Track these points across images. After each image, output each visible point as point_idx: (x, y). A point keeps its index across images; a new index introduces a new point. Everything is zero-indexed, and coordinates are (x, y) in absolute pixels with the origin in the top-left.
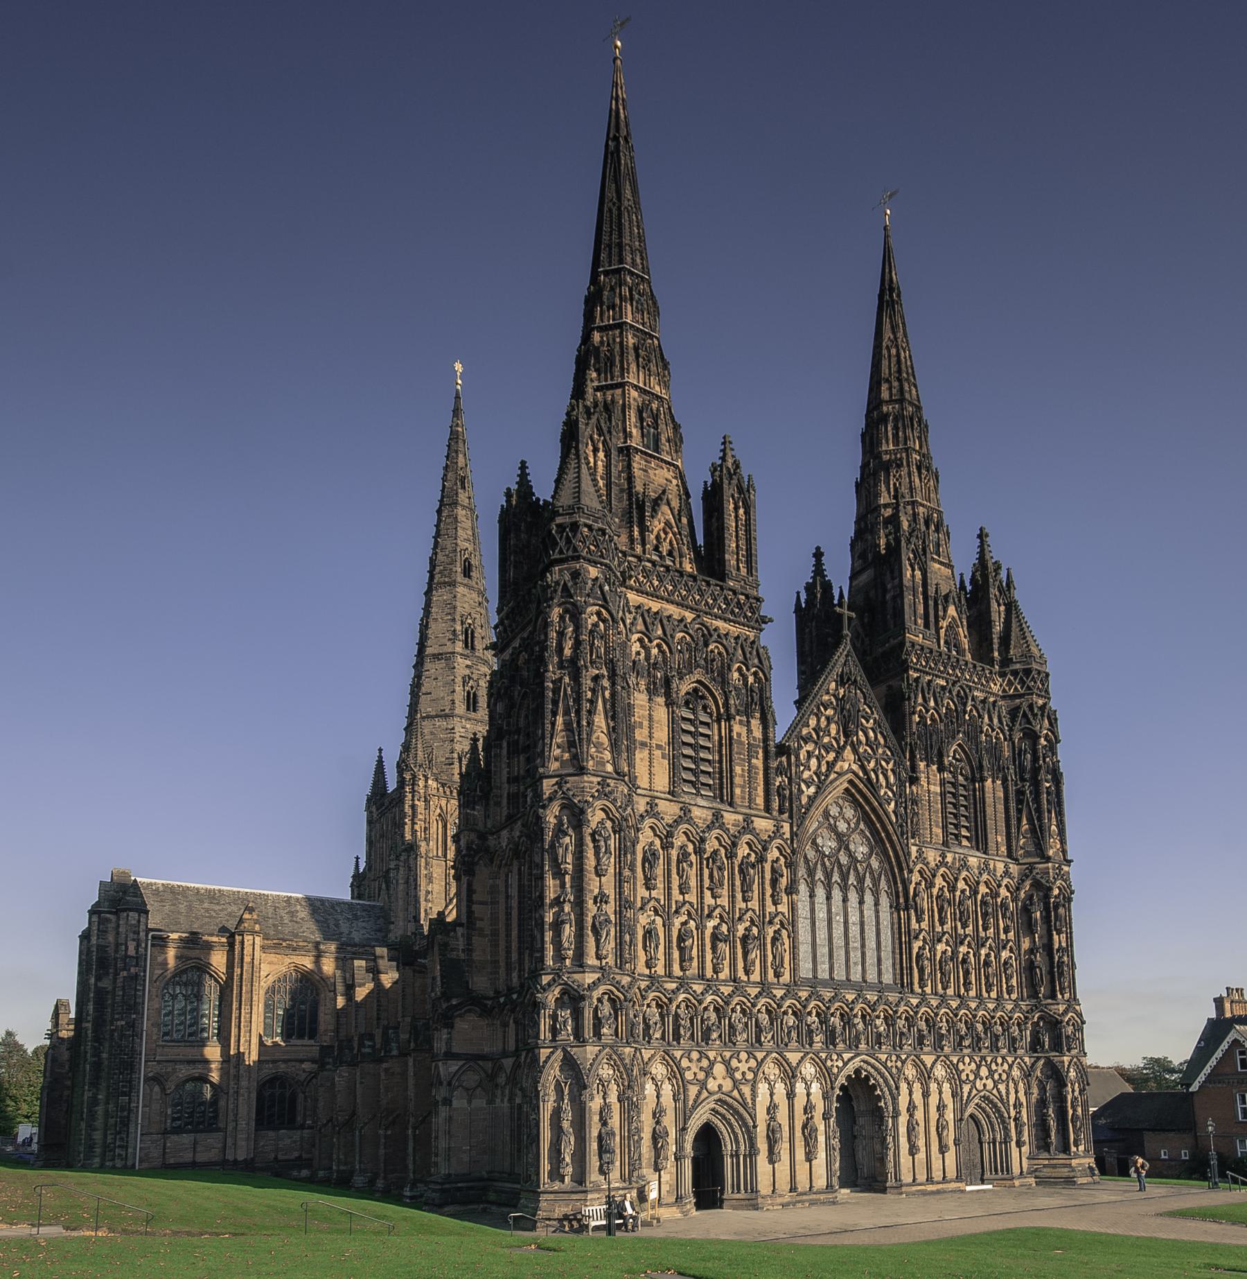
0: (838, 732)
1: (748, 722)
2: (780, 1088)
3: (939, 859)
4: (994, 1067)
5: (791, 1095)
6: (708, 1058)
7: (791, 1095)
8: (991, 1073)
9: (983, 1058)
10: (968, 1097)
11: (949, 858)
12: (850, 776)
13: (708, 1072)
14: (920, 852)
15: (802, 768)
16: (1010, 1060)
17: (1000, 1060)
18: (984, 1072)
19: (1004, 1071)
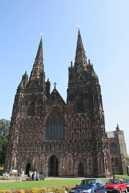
0: (53, 102)
1: (39, 104)
2: (38, 158)
3: (71, 116)
4: (83, 153)
5: (40, 159)
6: (26, 153)
7: (40, 159)
8: (82, 154)
9: (80, 151)
10: (76, 159)
11: (74, 116)
12: (54, 107)
13: (26, 155)
14: (67, 116)
15: (46, 108)
16: (87, 152)
17: (84, 152)
18: (80, 154)
19: (85, 154)
